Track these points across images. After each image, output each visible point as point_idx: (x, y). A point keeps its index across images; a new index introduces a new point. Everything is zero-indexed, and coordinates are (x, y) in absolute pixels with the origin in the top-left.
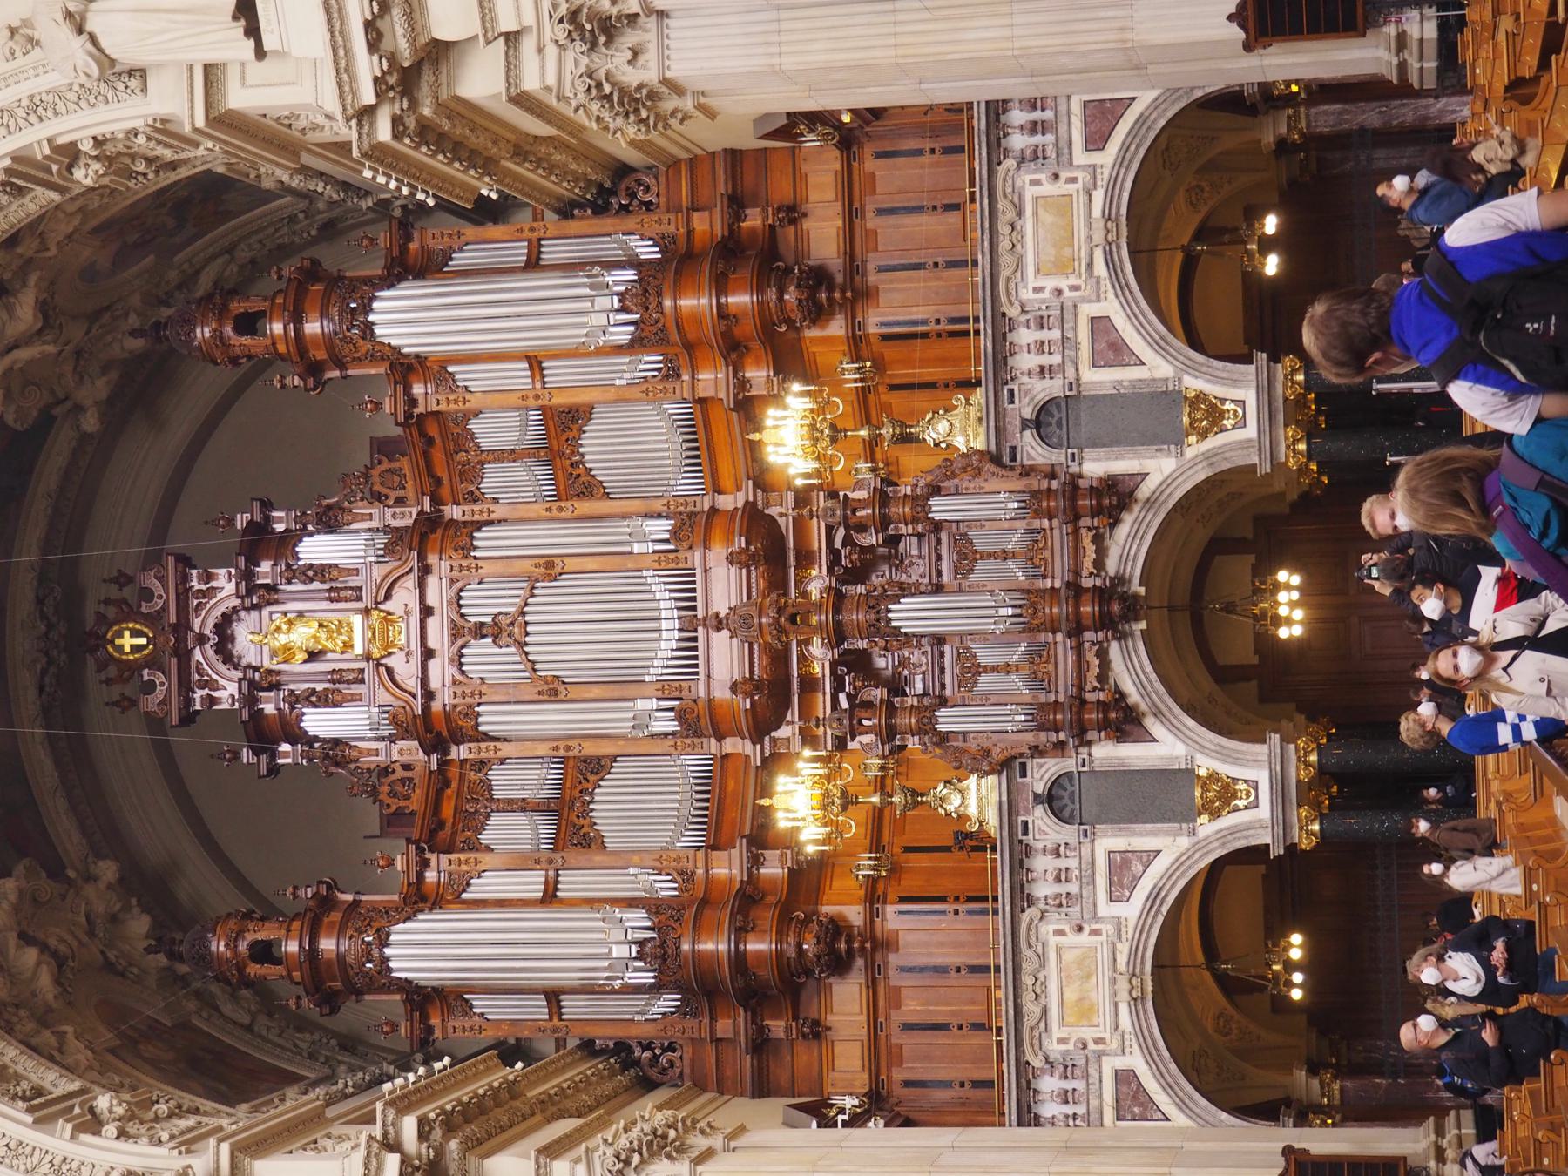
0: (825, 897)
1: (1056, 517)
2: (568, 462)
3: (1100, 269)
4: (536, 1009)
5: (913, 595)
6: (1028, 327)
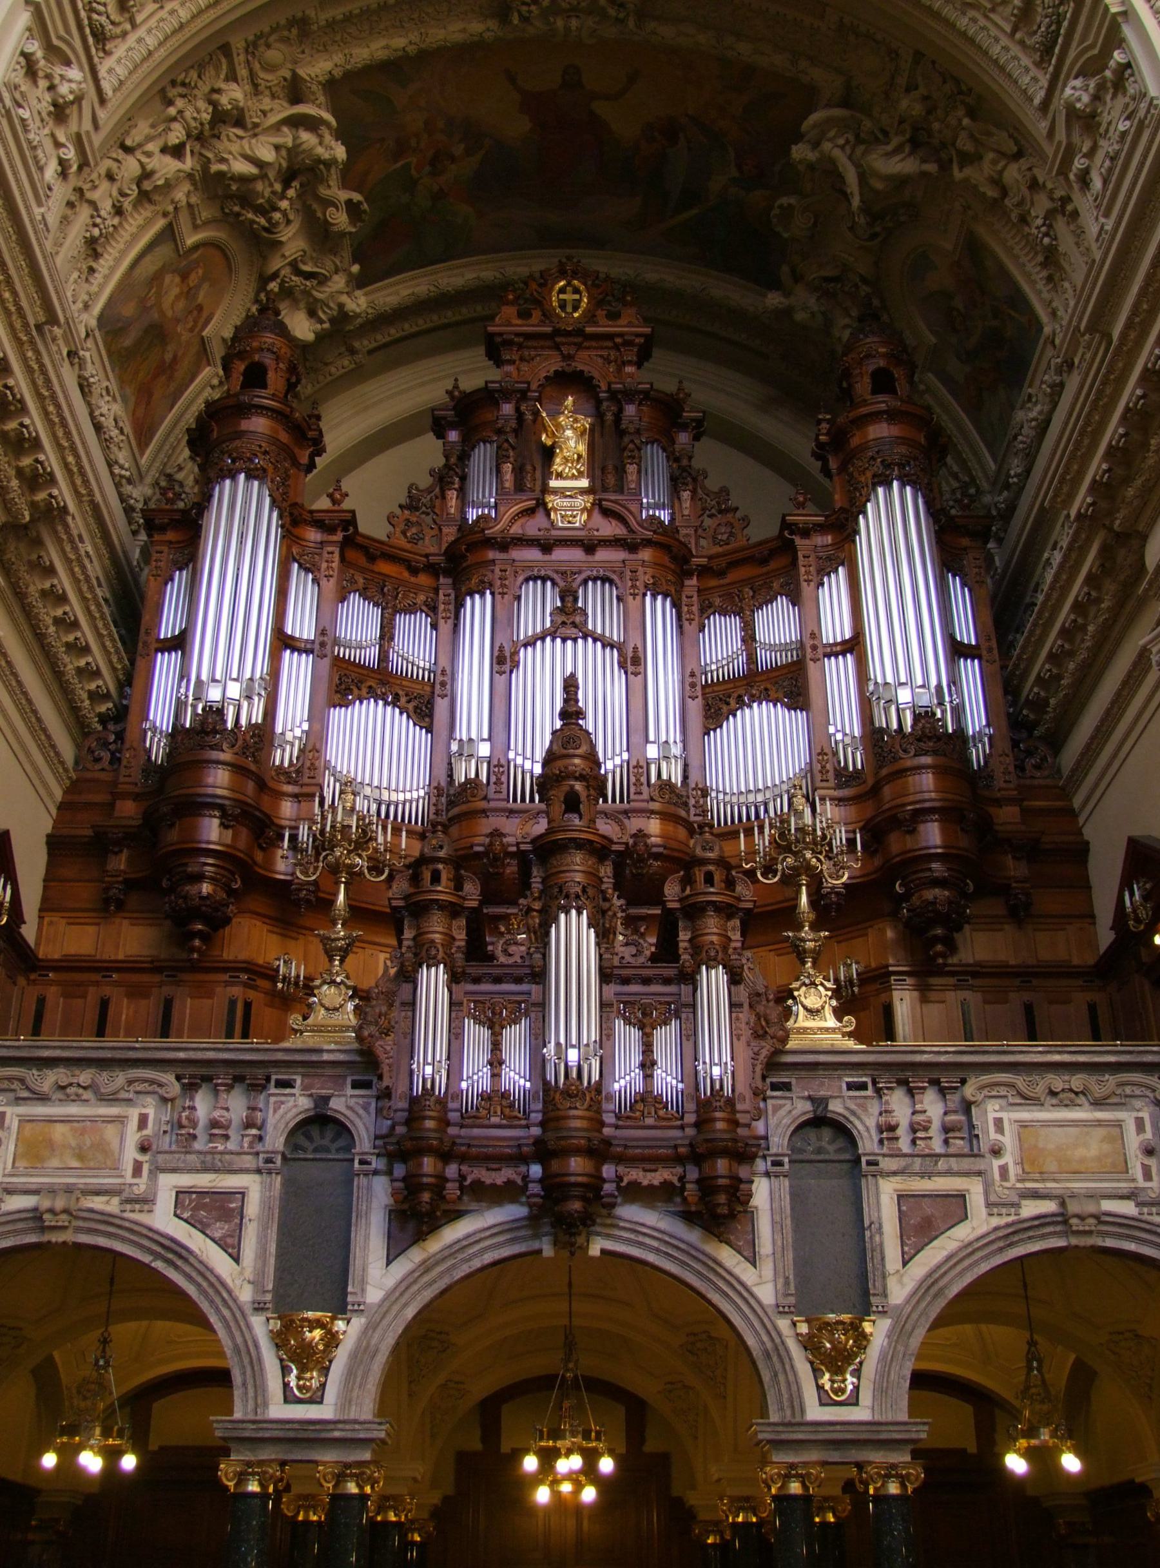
0: (258, 923)
1: (699, 1132)
2: (741, 691)
3: (1030, 1209)
4: (168, 628)
5: (598, 944)
6: (945, 1113)
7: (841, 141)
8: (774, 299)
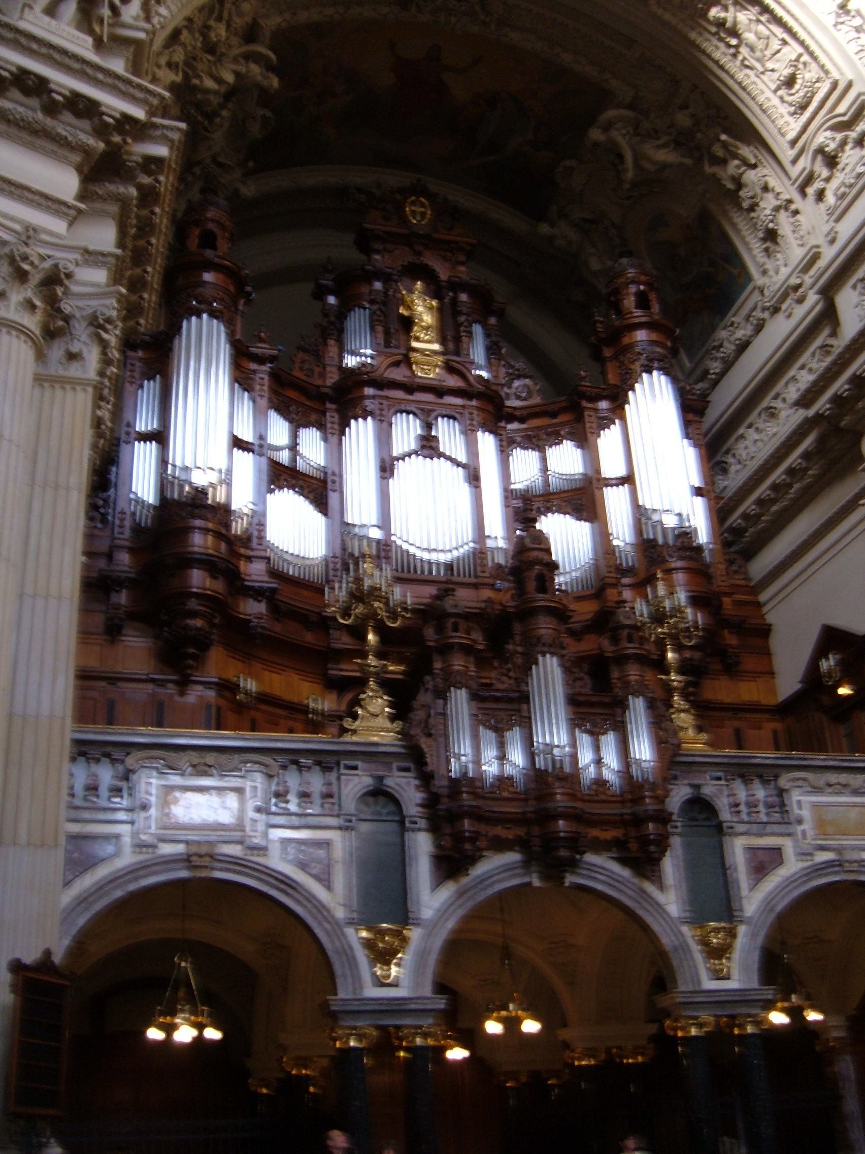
7: (624, 132)
8: (544, 229)
